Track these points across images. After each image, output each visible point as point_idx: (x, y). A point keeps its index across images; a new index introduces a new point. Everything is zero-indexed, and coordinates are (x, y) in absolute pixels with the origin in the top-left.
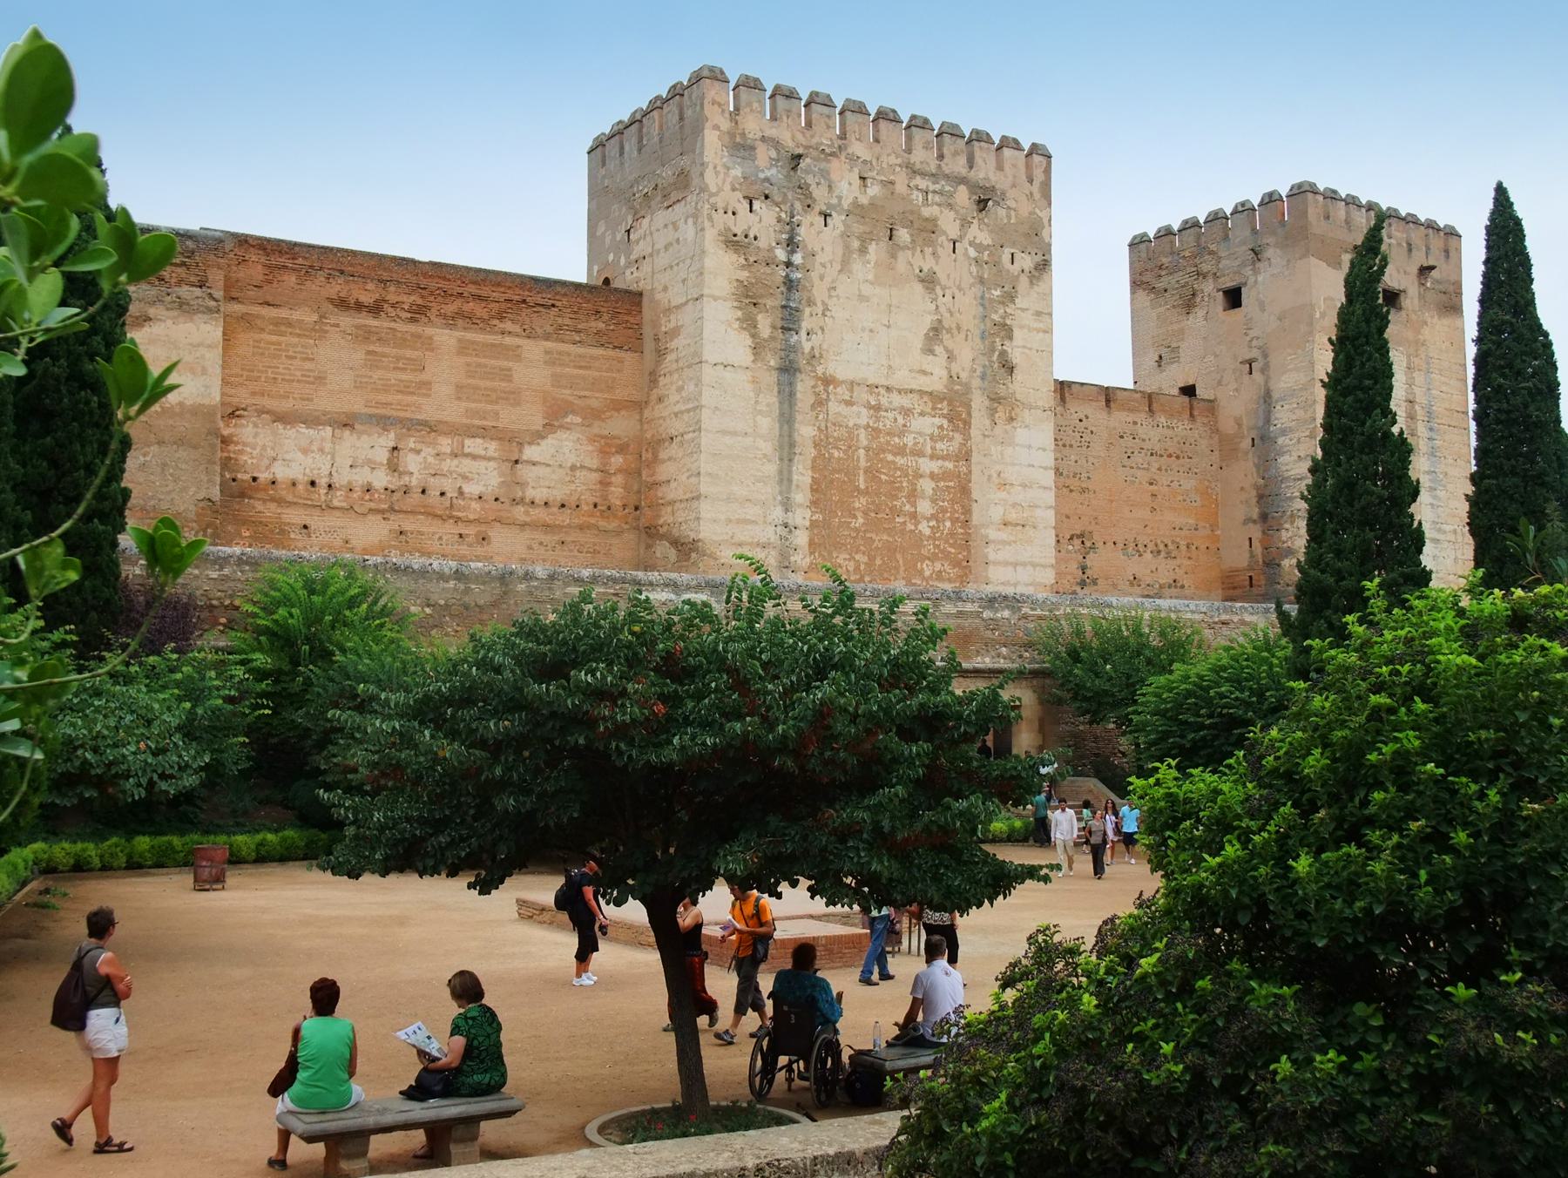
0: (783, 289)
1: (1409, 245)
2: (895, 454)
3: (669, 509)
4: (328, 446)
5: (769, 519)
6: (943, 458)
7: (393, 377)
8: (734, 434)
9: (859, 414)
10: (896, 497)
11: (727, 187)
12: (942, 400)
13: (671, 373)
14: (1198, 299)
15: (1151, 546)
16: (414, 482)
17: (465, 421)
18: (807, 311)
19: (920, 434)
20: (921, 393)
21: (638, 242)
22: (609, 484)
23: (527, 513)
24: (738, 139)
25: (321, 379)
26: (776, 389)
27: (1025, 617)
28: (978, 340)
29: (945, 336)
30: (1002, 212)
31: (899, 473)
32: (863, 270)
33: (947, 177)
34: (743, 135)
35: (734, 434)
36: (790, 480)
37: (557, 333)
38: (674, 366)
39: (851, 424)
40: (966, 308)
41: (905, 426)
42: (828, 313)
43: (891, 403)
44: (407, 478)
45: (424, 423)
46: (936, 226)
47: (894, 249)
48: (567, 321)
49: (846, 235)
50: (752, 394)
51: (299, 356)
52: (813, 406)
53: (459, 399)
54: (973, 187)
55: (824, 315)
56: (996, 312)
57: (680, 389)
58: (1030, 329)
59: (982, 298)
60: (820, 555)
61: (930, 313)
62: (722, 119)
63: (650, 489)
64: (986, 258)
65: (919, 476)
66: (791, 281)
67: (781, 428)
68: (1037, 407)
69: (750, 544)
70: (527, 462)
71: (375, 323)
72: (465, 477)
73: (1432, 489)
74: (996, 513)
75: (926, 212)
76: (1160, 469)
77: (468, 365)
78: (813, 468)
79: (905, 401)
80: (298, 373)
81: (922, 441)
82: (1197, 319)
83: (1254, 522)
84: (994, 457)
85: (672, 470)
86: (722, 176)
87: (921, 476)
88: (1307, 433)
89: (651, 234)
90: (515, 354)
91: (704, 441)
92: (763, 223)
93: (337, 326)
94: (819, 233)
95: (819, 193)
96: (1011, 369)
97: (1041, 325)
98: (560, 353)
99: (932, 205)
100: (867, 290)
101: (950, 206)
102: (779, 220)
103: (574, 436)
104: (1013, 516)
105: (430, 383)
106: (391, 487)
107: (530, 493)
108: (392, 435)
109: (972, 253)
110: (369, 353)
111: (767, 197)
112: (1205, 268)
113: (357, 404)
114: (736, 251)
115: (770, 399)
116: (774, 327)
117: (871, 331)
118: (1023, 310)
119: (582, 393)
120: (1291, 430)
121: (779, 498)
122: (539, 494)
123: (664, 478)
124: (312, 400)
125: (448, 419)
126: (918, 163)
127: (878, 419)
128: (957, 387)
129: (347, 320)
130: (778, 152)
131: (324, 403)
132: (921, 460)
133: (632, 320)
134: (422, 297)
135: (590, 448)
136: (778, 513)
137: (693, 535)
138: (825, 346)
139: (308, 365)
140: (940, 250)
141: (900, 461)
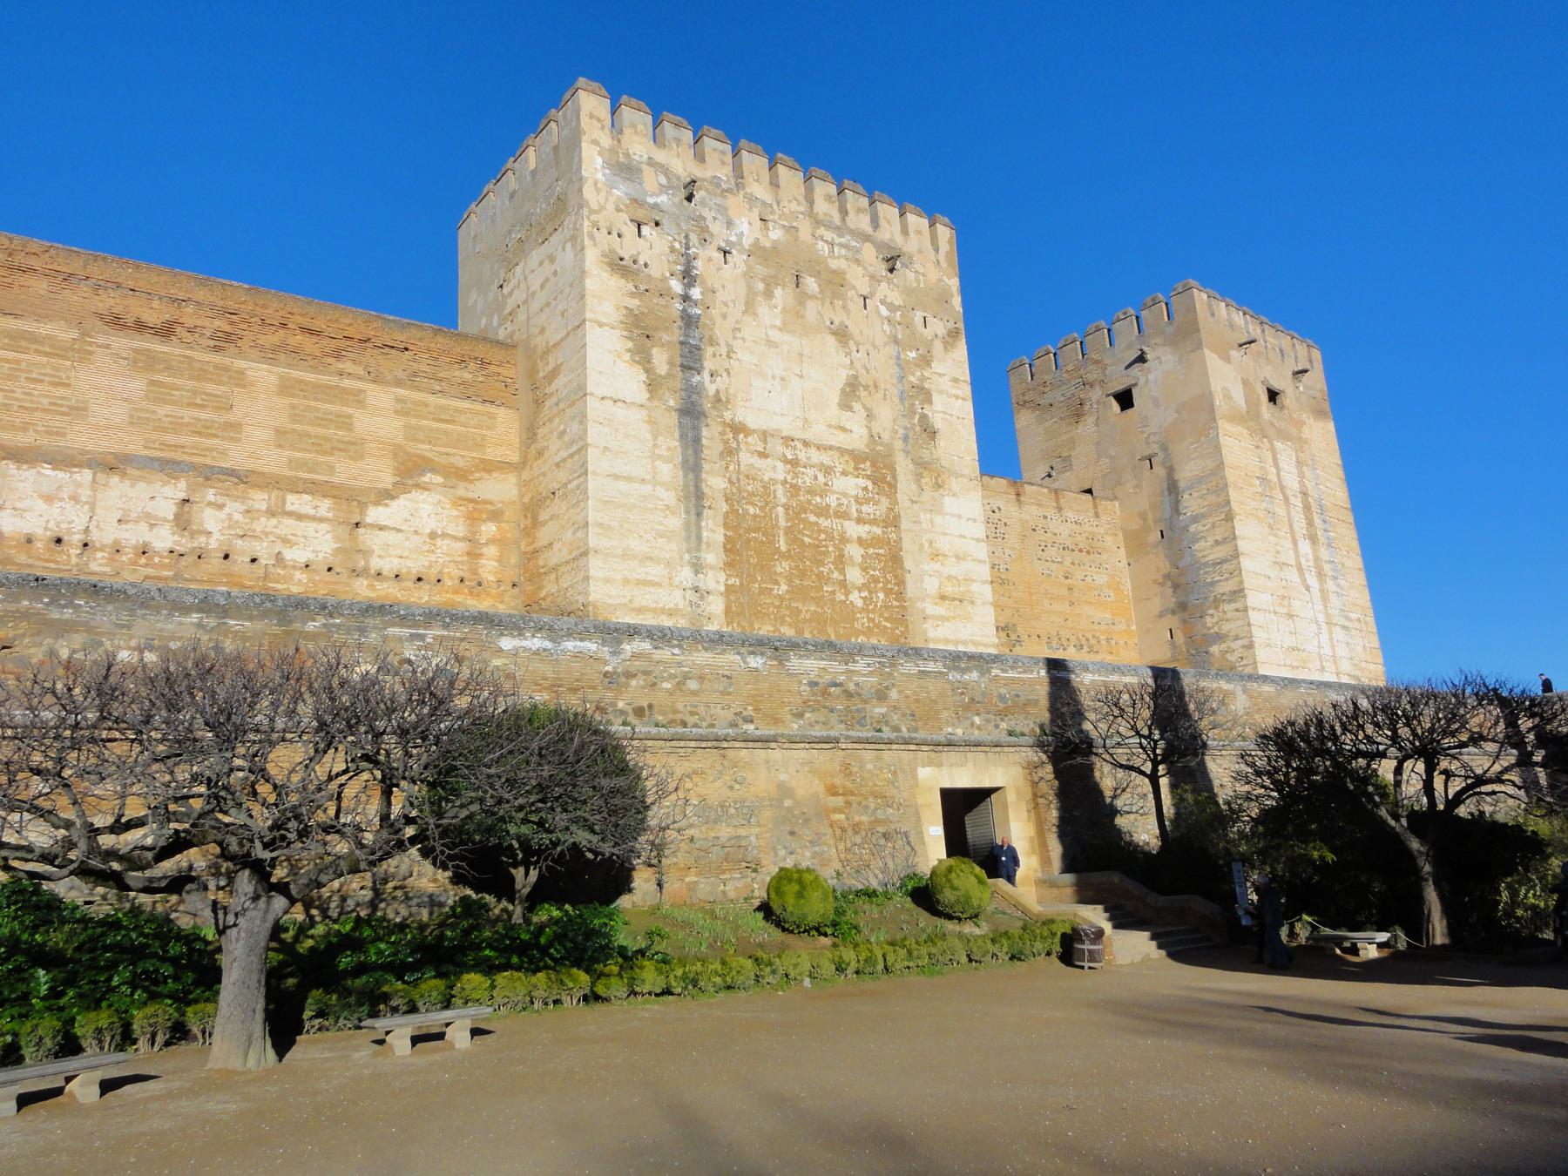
0: (679, 323)
1: (1281, 351)
2: (818, 515)
3: (553, 576)
4: (85, 494)
5: (676, 581)
6: (873, 522)
7: (187, 414)
8: (629, 479)
9: (774, 468)
10: (821, 563)
11: (611, 207)
12: (867, 458)
13: (550, 420)
14: (1086, 407)
15: (1073, 639)
16: (213, 544)
17: (288, 473)
18: (709, 351)
19: (845, 495)
20: (842, 451)
21: (510, 294)
22: (480, 555)
23: (372, 587)
24: (622, 159)
25: (79, 410)
26: (677, 434)
27: (996, 679)
28: (897, 400)
29: (863, 393)
30: (911, 275)
31: (823, 536)
32: (770, 315)
33: (852, 233)
34: (627, 155)
35: (629, 479)
36: (699, 538)
37: (411, 379)
38: (555, 410)
39: (766, 478)
40: (881, 364)
41: (826, 484)
42: (734, 356)
43: (809, 458)
44: (203, 539)
45: (231, 473)
46: (844, 279)
47: (802, 298)
48: (426, 368)
49: (749, 275)
50: (649, 436)
51: (47, 379)
52: (721, 454)
53: (280, 446)
54: (880, 246)
55: (729, 357)
56: (913, 374)
57: (562, 434)
58: (950, 396)
59: (898, 358)
60: (739, 622)
61: (845, 367)
62: (602, 135)
63: (529, 560)
64: (898, 319)
65: (844, 540)
66: (689, 316)
67: (685, 476)
68: (963, 476)
69: (654, 610)
70: (372, 526)
71: (165, 349)
72: (285, 541)
73: (1335, 578)
74: (932, 586)
75: (834, 264)
76: (1073, 563)
77: (293, 407)
78: (726, 525)
79: (825, 458)
80: (45, 401)
81: (846, 502)
82: (1087, 427)
83: (1173, 612)
84: (924, 526)
85: (555, 536)
86: (603, 194)
87: (848, 541)
88: (1223, 516)
89: (526, 279)
90: (357, 399)
91: (591, 485)
92: (654, 250)
93: (107, 347)
94: (719, 269)
95: (716, 228)
96: (931, 433)
97: (959, 392)
98: (415, 403)
99: (839, 257)
100: (775, 335)
101: (858, 262)
102: (672, 249)
103: (434, 497)
104: (950, 589)
105: (240, 425)
106: (181, 550)
107: (375, 563)
108: (182, 484)
109: (884, 311)
110: (152, 383)
111: (657, 224)
112: (1091, 377)
113: (133, 444)
114: (623, 276)
115: (671, 443)
116: (671, 363)
117: (782, 379)
118: (941, 375)
119: (444, 450)
120: (1203, 516)
121: (687, 557)
122: (388, 565)
123: (545, 542)
124: (64, 435)
125: (265, 470)
126: (820, 213)
127: (796, 475)
128: (879, 448)
129: (123, 343)
130: (669, 179)
131: (80, 438)
132: (847, 523)
133: (506, 373)
134: (232, 323)
135: (455, 513)
136: (686, 575)
137: (581, 599)
138: (731, 391)
139: (60, 392)
140: (851, 305)
141: (824, 523)
